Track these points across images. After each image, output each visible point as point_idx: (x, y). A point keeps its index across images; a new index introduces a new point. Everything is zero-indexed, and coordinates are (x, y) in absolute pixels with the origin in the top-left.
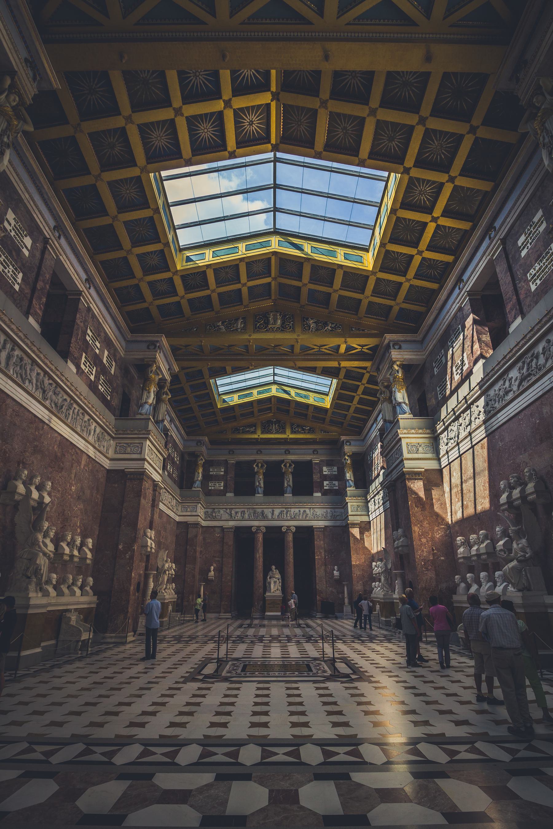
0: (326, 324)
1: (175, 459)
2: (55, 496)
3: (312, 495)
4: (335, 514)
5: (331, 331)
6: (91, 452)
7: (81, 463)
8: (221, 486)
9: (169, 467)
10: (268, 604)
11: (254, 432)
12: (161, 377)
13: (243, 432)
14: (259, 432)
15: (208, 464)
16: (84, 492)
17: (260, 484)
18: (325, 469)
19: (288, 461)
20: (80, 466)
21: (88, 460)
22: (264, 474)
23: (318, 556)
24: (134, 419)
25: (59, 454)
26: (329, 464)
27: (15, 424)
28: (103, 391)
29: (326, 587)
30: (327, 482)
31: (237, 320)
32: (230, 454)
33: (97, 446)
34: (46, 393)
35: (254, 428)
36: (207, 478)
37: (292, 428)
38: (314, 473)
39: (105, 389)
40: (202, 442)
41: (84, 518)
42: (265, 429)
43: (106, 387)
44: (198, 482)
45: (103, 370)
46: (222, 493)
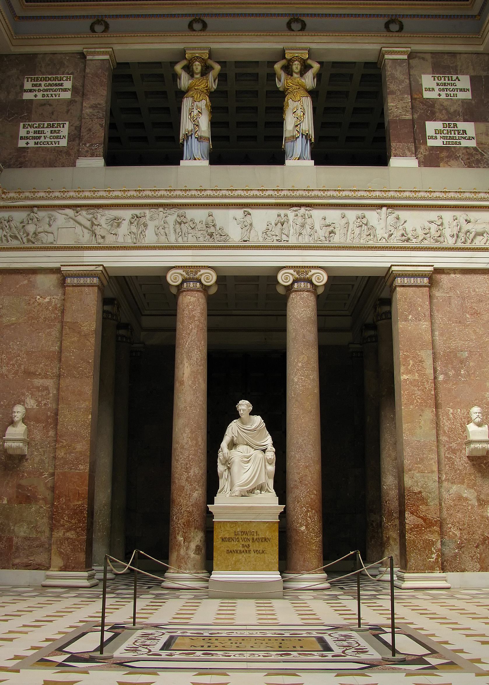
4: (469, 227)
10: (223, 540)
22: (212, 95)
23: (409, 372)
30: (438, 125)
32: (93, 30)
38: (393, 93)
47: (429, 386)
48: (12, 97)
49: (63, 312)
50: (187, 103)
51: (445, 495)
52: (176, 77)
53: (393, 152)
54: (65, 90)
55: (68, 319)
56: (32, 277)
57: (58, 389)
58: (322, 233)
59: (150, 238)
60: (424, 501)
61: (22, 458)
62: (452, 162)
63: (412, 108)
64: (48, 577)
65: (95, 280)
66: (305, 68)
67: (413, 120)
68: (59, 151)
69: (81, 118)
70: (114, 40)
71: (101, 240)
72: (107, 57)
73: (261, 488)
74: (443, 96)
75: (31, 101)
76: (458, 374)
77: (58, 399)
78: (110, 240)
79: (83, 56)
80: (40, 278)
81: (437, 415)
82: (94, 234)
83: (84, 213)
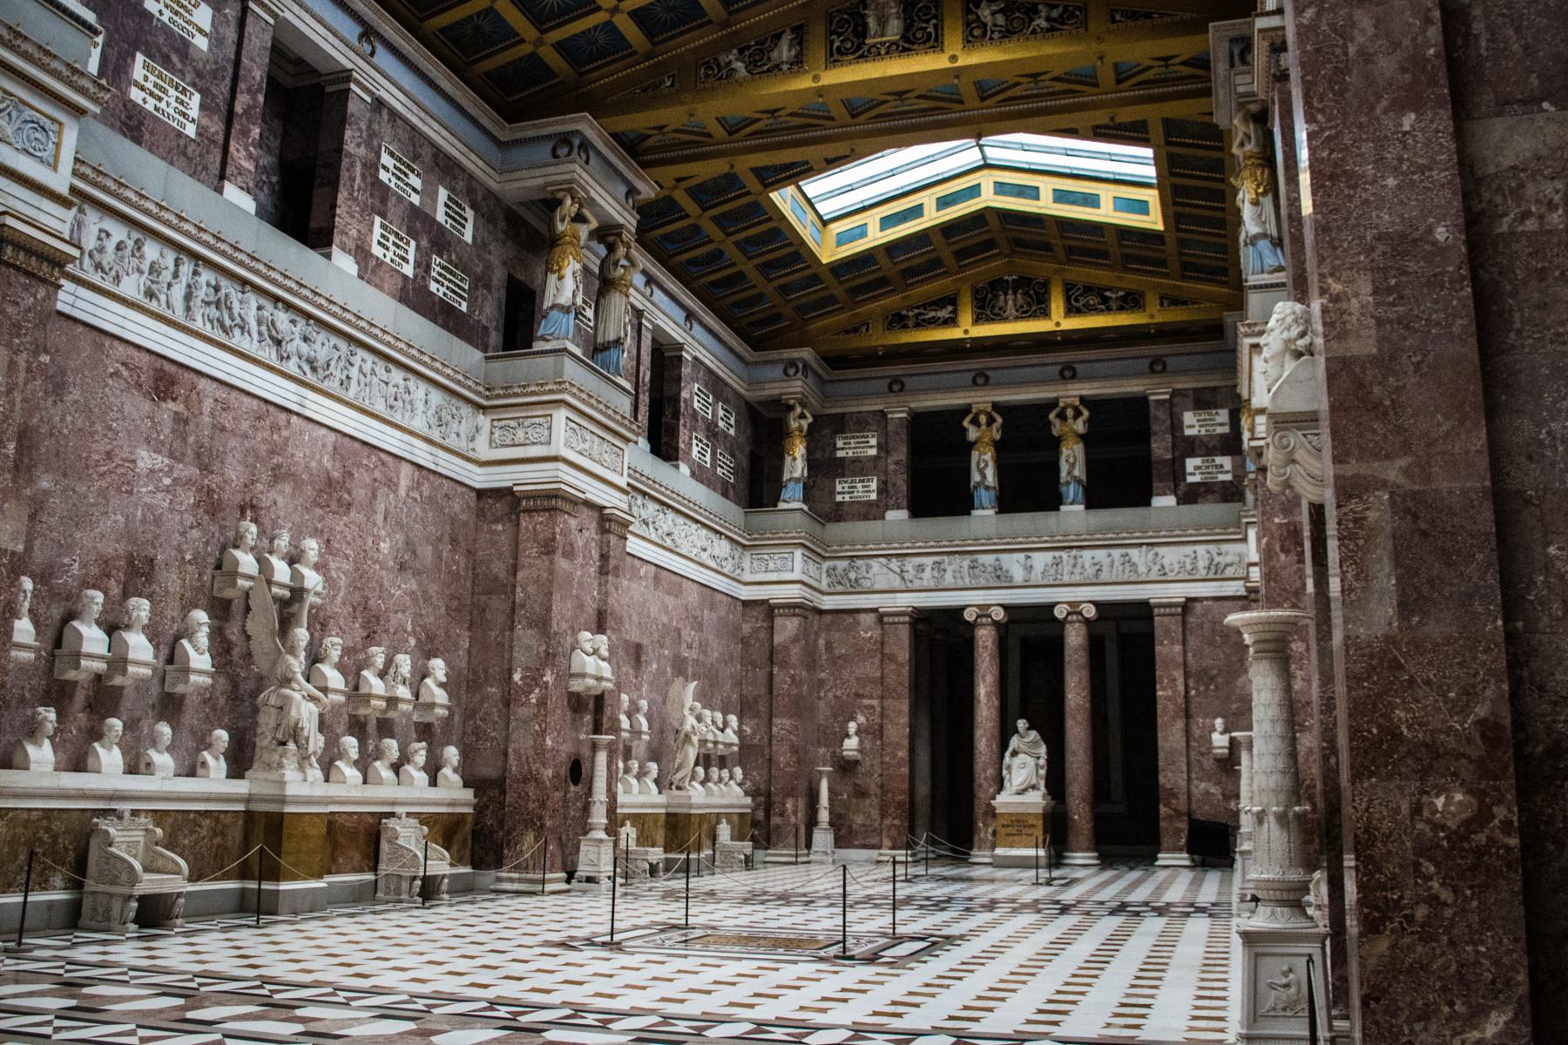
0: (1032, 11)
1: (721, 424)
2: (339, 568)
3: (1148, 504)
5: (1048, 30)
6: (422, 454)
7: (396, 485)
8: (867, 490)
9: (695, 450)
11: (951, 322)
12: (594, 224)
13: (918, 325)
14: (966, 317)
15: (824, 429)
16: (414, 553)
17: (984, 477)
18: (1189, 418)
19: (1069, 401)
20: (395, 492)
21: (417, 473)
22: (999, 447)
24: (529, 354)
25: (336, 475)
26: (1203, 401)
27: (223, 429)
28: (445, 294)
29: (1189, 780)
30: (1197, 461)
31: (778, 37)
32: (891, 390)
33: (436, 436)
34: (284, 343)
35: (950, 308)
36: (824, 468)
37: (1068, 300)
38: (1156, 434)
39: (448, 288)
40: (801, 366)
41: (423, 612)
42: (982, 307)
43: (450, 281)
44: (791, 485)
45: (438, 241)
46: (871, 512)
47: (1180, 700)
48: (827, 455)
49: (882, 644)
50: (975, 455)
51: (1195, 791)
52: (965, 430)
53: (1155, 491)
54: (871, 447)
55: (887, 651)
56: (856, 616)
57: (882, 708)
58: (1091, 571)
59: (949, 579)
60: (1174, 795)
61: (856, 763)
62: (1210, 497)
63: (1174, 445)
64: (881, 855)
65: (907, 619)
66: (1078, 414)
67: (1173, 460)
68: (870, 504)
69: (886, 472)
70: (908, 398)
71: (909, 585)
72: (904, 415)
73: (1034, 787)
74: (1203, 432)
75: (843, 459)
76: (1207, 689)
77: (882, 716)
78: (917, 584)
79: (883, 414)
80: (862, 617)
81: (1187, 724)
82: (903, 579)
83: (894, 560)
